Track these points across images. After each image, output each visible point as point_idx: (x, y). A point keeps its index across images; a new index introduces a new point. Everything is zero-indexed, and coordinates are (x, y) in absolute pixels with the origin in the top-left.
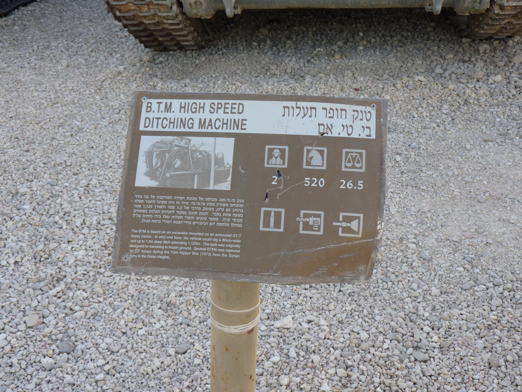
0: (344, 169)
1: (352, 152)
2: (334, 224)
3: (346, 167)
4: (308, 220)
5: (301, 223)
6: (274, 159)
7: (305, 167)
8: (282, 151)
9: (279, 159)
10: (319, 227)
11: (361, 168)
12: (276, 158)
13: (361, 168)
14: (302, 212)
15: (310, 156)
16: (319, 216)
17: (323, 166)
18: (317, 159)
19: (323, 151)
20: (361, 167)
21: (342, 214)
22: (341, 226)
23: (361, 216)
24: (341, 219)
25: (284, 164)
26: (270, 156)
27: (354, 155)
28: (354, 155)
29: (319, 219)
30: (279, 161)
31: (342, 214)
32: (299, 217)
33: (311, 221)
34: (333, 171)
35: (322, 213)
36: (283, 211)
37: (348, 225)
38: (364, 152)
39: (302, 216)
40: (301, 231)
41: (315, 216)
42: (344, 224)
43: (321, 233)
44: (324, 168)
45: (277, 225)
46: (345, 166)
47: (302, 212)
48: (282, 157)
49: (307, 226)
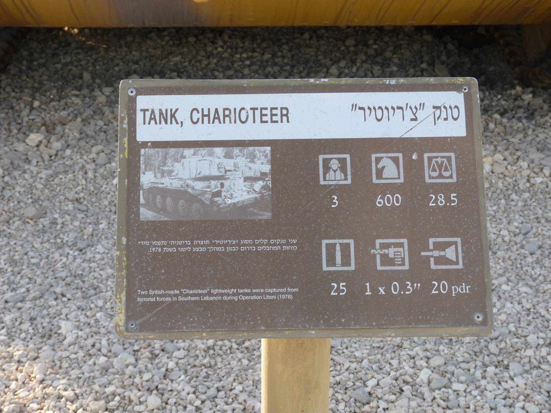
0: (428, 180)
1: (437, 157)
2: (423, 254)
3: (430, 177)
4: (386, 251)
5: (378, 257)
6: (332, 172)
7: (375, 181)
8: (342, 162)
9: (338, 172)
10: (403, 260)
11: (451, 177)
12: (335, 171)
13: (451, 177)
14: (378, 242)
15: (380, 166)
16: (401, 245)
17: (399, 178)
18: (391, 170)
19: (398, 158)
20: (451, 176)
21: (431, 240)
22: (432, 256)
23: (459, 240)
24: (431, 247)
25: (346, 179)
26: (327, 169)
27: (439, 160)
28: (439, 160)
29: (401, 249)
30: (339, 175)
31: (431, 240)
32: (375, 248)
33: (391, 252)
34: (414, 185)
35: (405, 241)
36: (351, 242)
37: (442, 253)
38: (452, 155)
39: (378, 246)
40: (379, 268)
41: (397, 245)
42: (436, 253)
43: (406, 267)
44: (402, 180)
45: (346, 262)
46: (430, 176)
47: (378, 242)
48: (343, 169)
49: (387, 260)
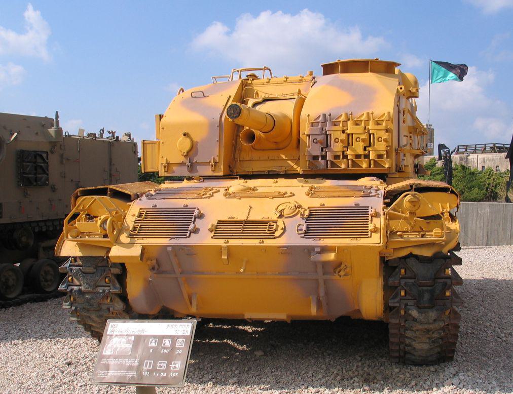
8: (156, 341)
16: (165, 363)
33: (162, 364)
41: (164, 363)
42: (173, 365)
48: (155, 343)
49: (160, 367)
